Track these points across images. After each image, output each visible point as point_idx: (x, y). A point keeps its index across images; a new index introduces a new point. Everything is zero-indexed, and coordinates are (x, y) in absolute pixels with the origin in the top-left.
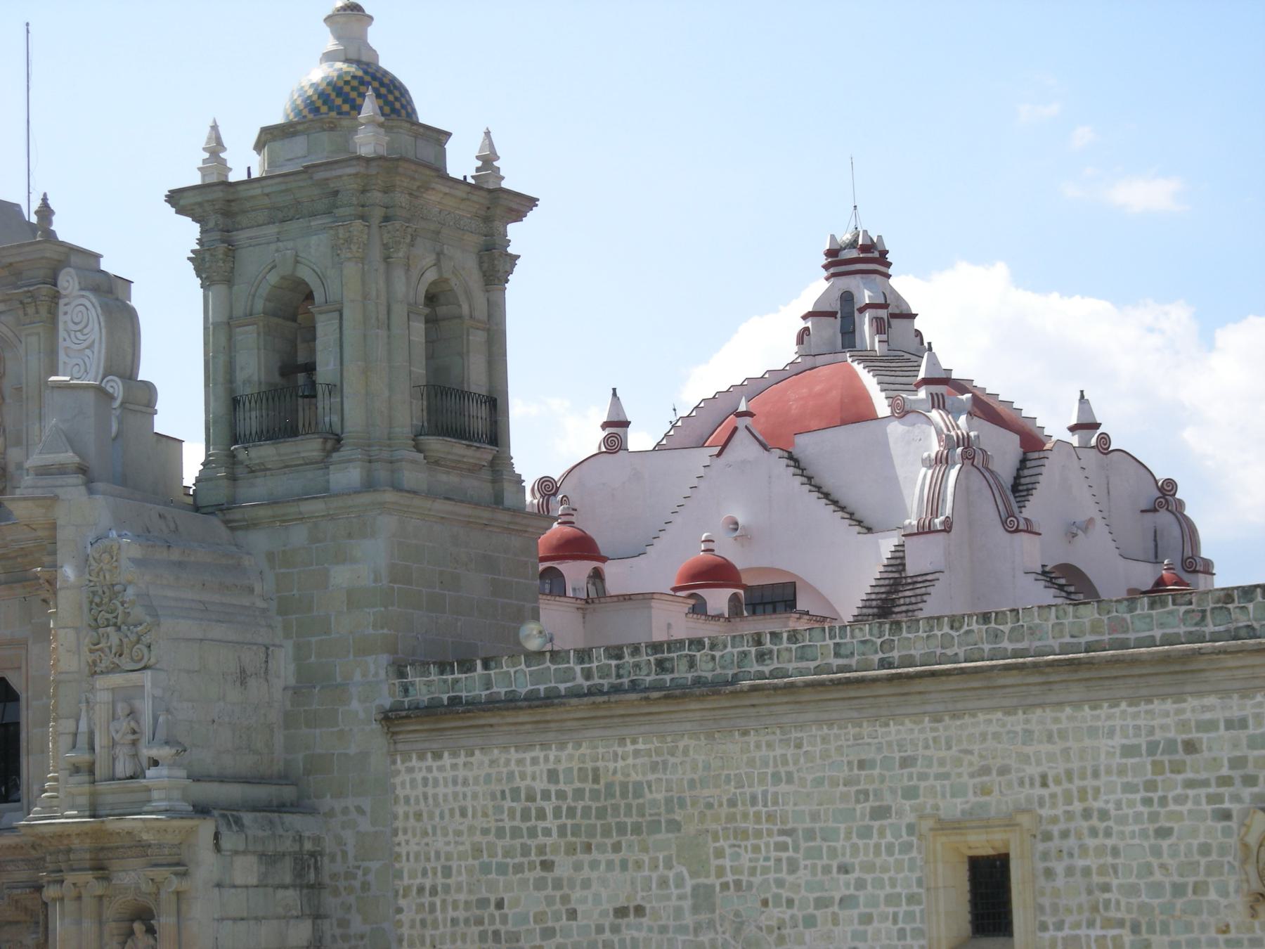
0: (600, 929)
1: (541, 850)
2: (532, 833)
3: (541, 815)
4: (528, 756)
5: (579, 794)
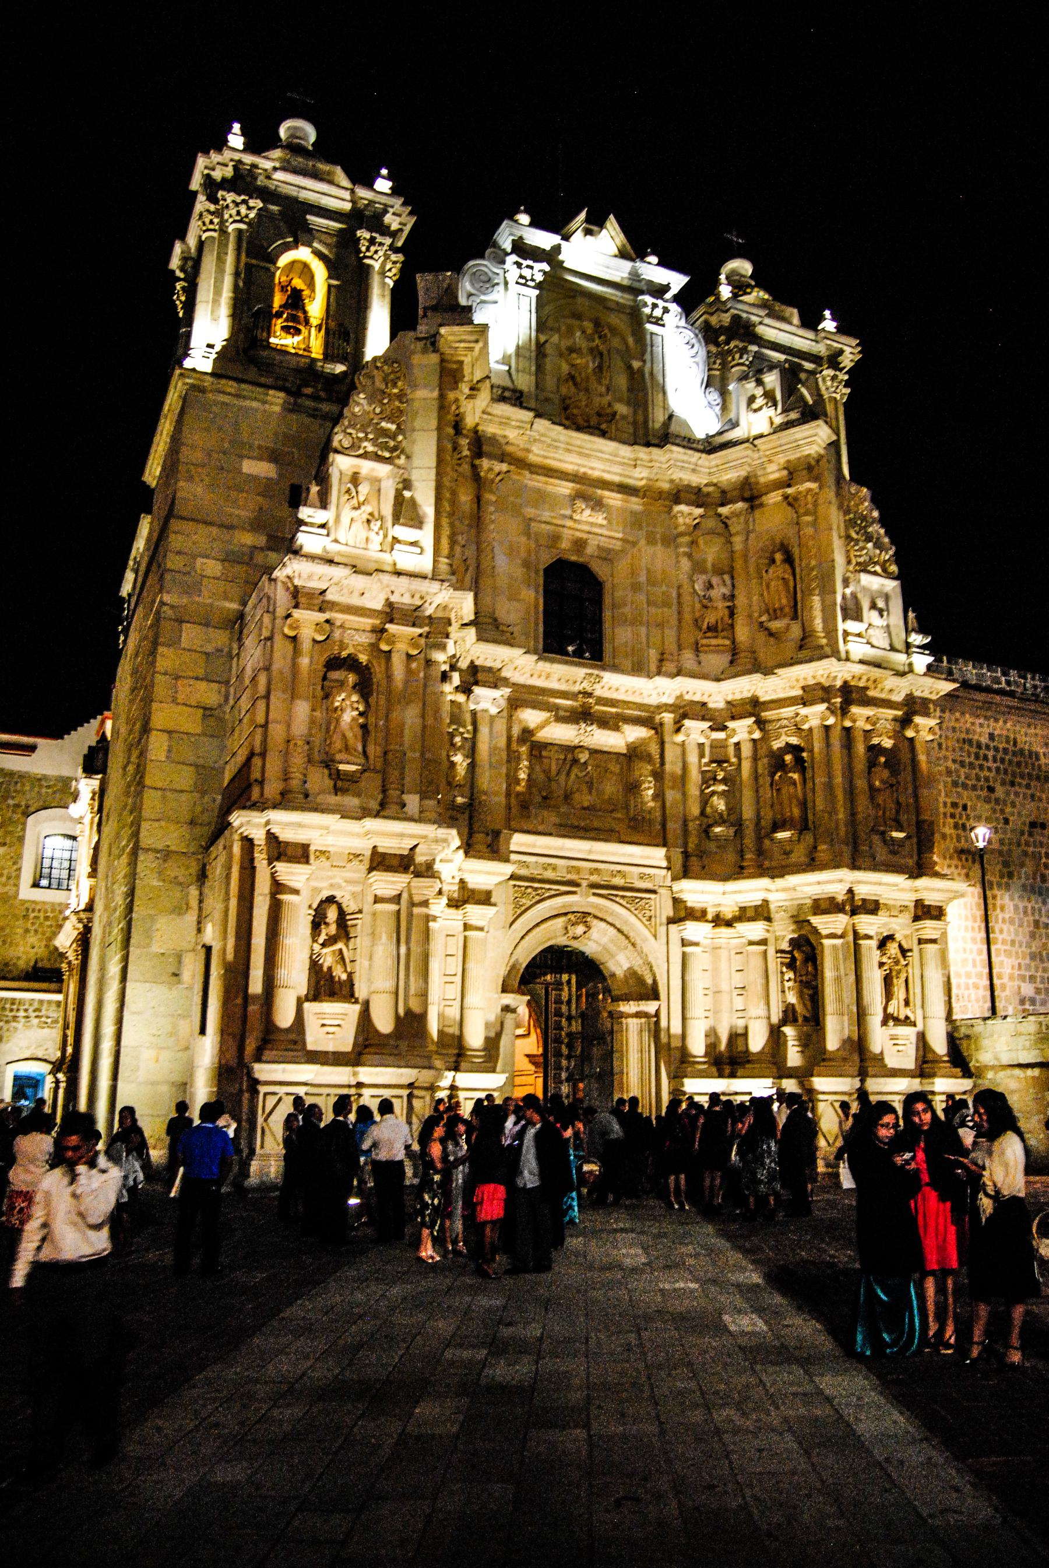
0: (1022, 833)
1: (987, 779)
2: (981, 767)
3: (986, 758)
4: (978, 721)
5: (1005, 750)
